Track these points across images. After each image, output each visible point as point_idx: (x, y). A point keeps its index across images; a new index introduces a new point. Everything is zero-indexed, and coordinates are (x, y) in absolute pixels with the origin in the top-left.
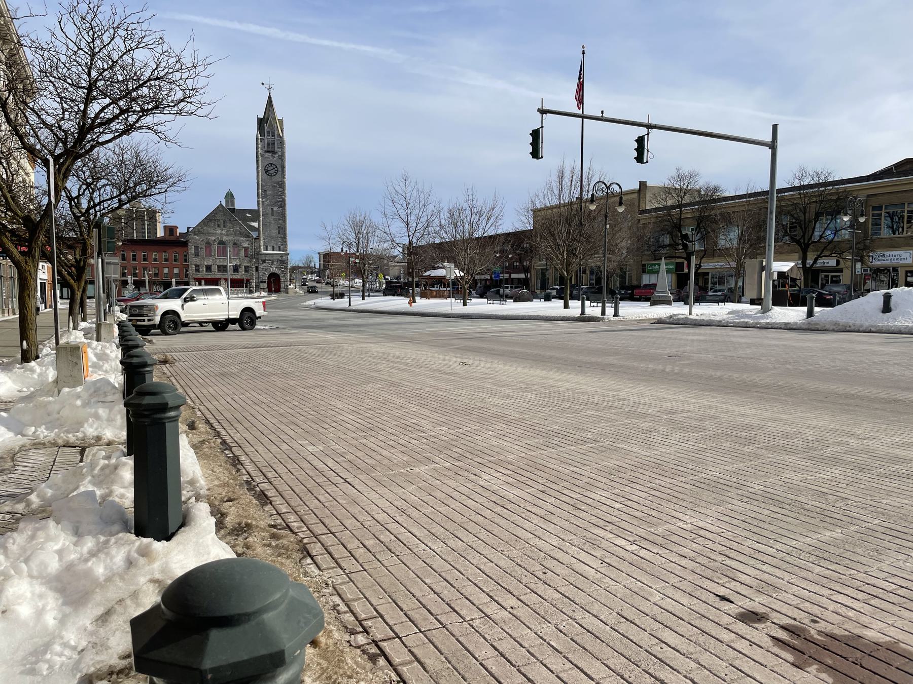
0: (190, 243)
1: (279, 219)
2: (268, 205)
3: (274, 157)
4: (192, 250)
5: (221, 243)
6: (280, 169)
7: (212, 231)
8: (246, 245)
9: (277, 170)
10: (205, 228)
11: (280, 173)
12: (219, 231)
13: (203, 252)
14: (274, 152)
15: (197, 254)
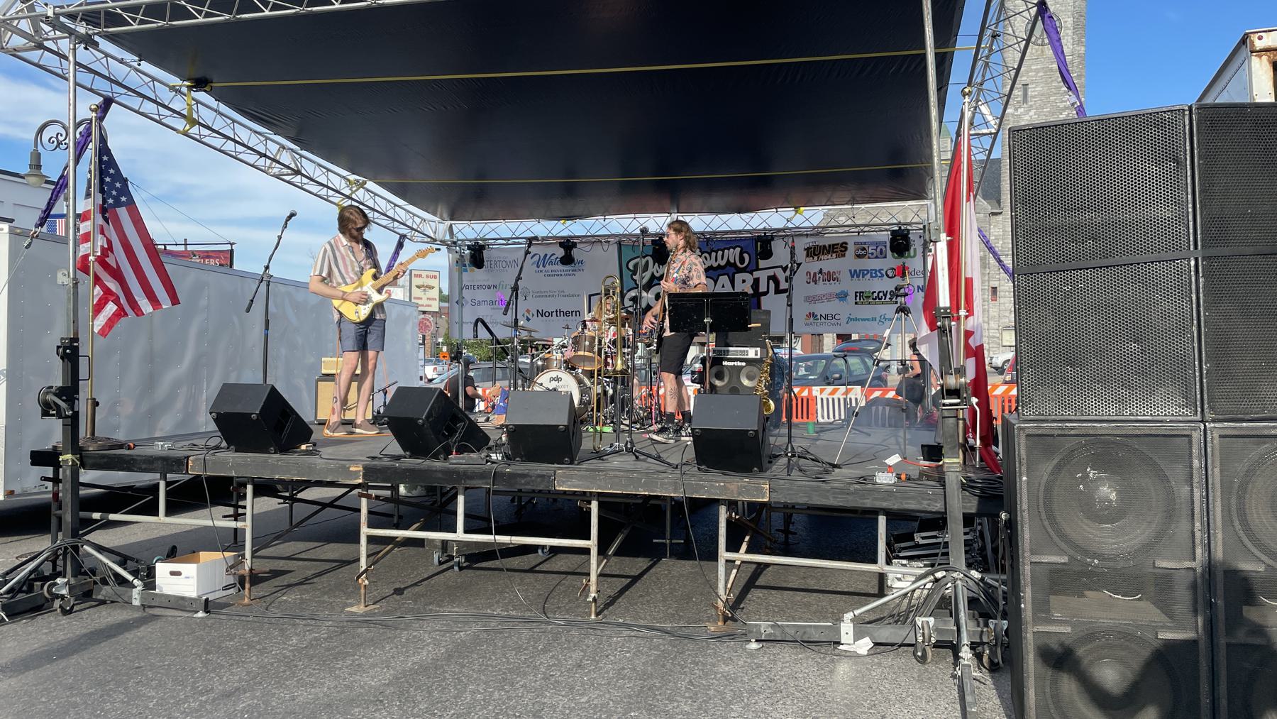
11: (1070, 32)
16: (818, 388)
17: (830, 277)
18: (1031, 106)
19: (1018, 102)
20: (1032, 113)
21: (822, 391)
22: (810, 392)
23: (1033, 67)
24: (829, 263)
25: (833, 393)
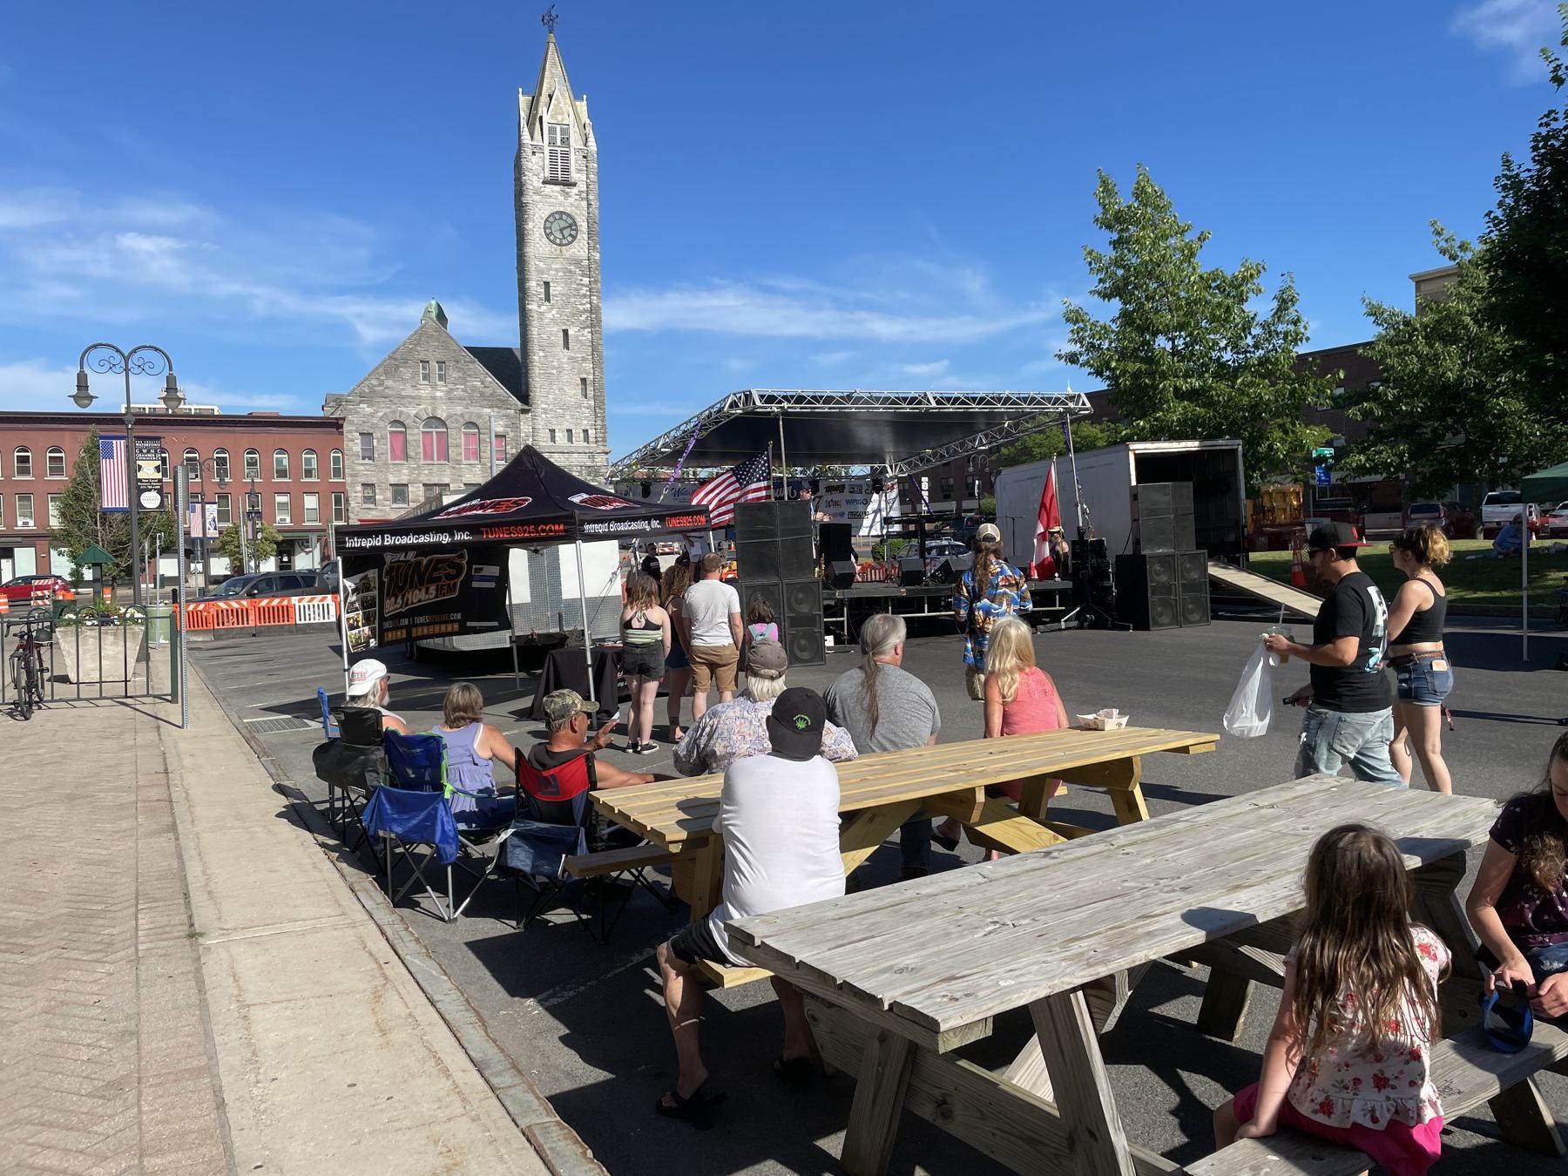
0: (352, 423)
1: (584, 359)
2: (553, 320)
3: (567, 195)
4: (353, 444)
5: (434, 420)
6: (583, 225)
7: (409, 391)
8: (498, 427)
9: (576, 230)
10: (389, 383)
11: (586, 237)
12: (425, 391)
13: (382, 446)
14: (569, 184)
15: (369, 454)
16: (297, 598)
17: (836, 504)
18: (553, 305)
19: (541, 299)
20: (554, 312)
21: (300, 601)
22: (289, 601)
23: (553, 266)
24: (835, 496)
25: (311, 601)
